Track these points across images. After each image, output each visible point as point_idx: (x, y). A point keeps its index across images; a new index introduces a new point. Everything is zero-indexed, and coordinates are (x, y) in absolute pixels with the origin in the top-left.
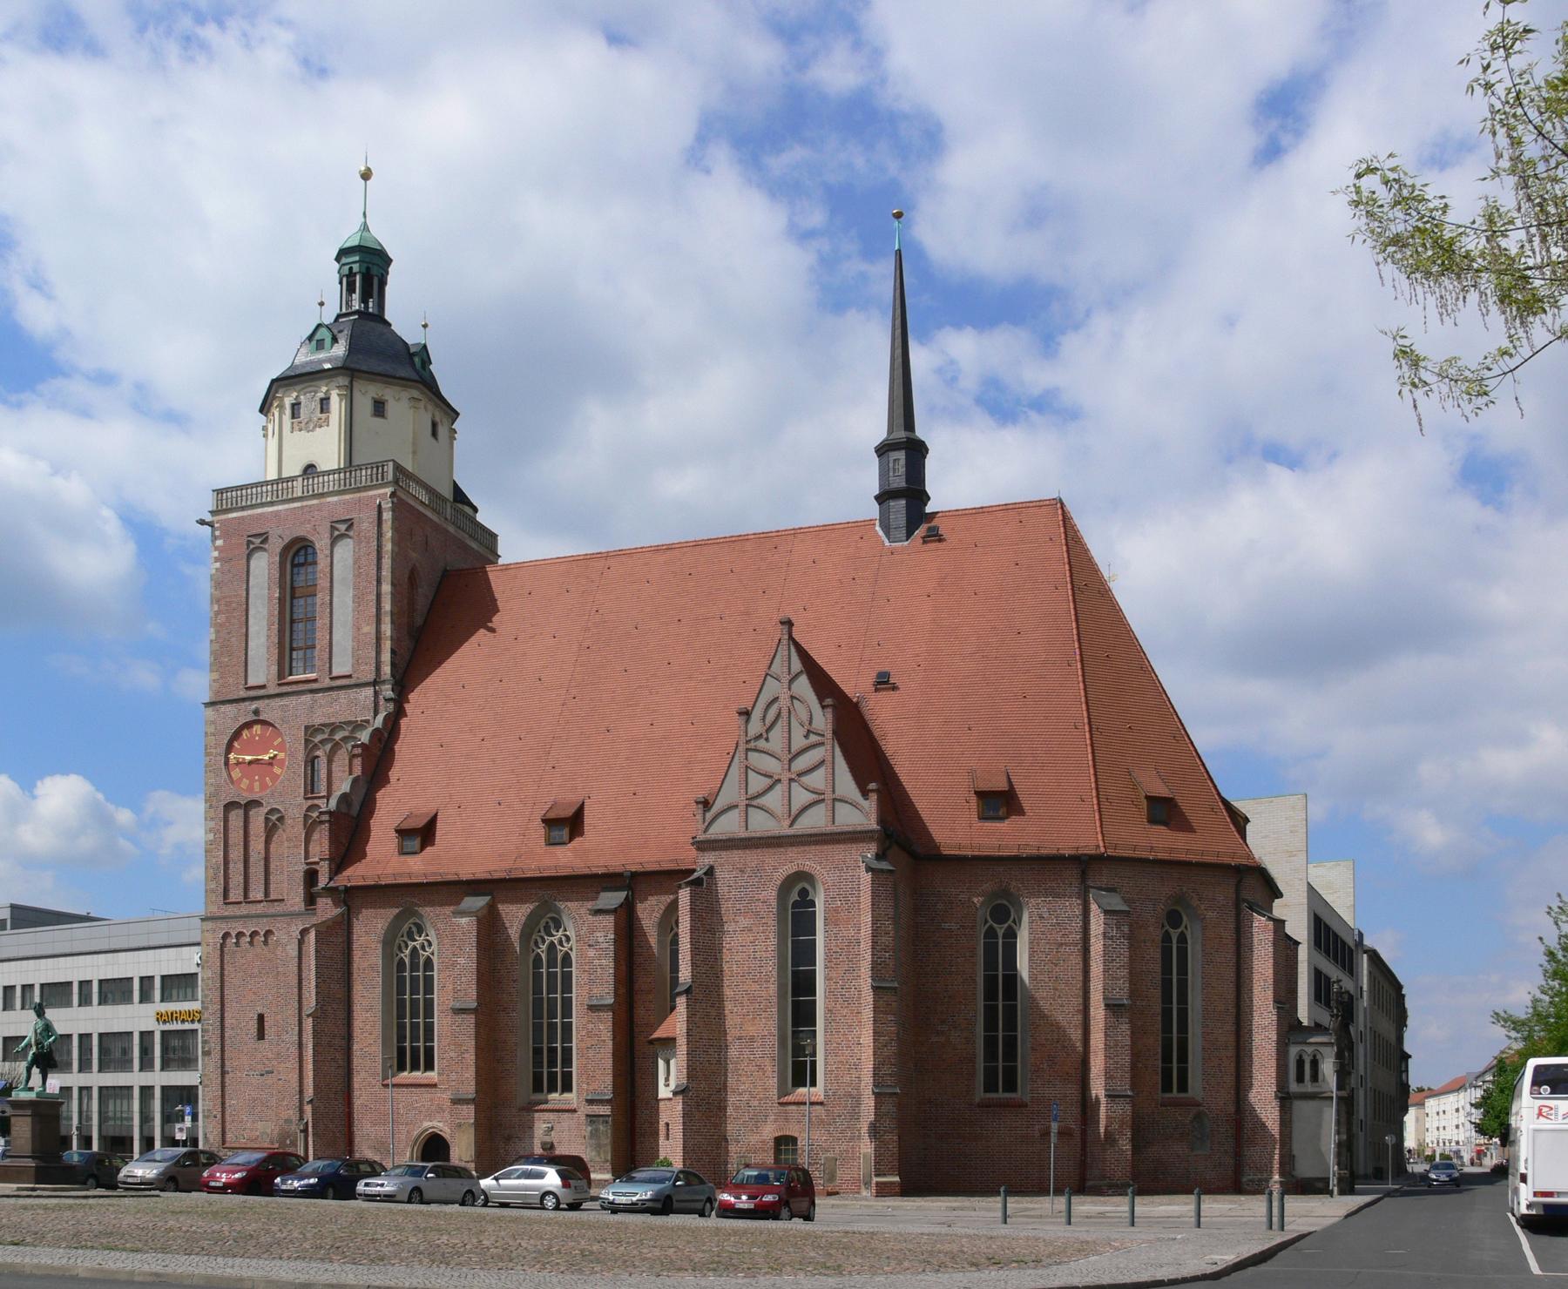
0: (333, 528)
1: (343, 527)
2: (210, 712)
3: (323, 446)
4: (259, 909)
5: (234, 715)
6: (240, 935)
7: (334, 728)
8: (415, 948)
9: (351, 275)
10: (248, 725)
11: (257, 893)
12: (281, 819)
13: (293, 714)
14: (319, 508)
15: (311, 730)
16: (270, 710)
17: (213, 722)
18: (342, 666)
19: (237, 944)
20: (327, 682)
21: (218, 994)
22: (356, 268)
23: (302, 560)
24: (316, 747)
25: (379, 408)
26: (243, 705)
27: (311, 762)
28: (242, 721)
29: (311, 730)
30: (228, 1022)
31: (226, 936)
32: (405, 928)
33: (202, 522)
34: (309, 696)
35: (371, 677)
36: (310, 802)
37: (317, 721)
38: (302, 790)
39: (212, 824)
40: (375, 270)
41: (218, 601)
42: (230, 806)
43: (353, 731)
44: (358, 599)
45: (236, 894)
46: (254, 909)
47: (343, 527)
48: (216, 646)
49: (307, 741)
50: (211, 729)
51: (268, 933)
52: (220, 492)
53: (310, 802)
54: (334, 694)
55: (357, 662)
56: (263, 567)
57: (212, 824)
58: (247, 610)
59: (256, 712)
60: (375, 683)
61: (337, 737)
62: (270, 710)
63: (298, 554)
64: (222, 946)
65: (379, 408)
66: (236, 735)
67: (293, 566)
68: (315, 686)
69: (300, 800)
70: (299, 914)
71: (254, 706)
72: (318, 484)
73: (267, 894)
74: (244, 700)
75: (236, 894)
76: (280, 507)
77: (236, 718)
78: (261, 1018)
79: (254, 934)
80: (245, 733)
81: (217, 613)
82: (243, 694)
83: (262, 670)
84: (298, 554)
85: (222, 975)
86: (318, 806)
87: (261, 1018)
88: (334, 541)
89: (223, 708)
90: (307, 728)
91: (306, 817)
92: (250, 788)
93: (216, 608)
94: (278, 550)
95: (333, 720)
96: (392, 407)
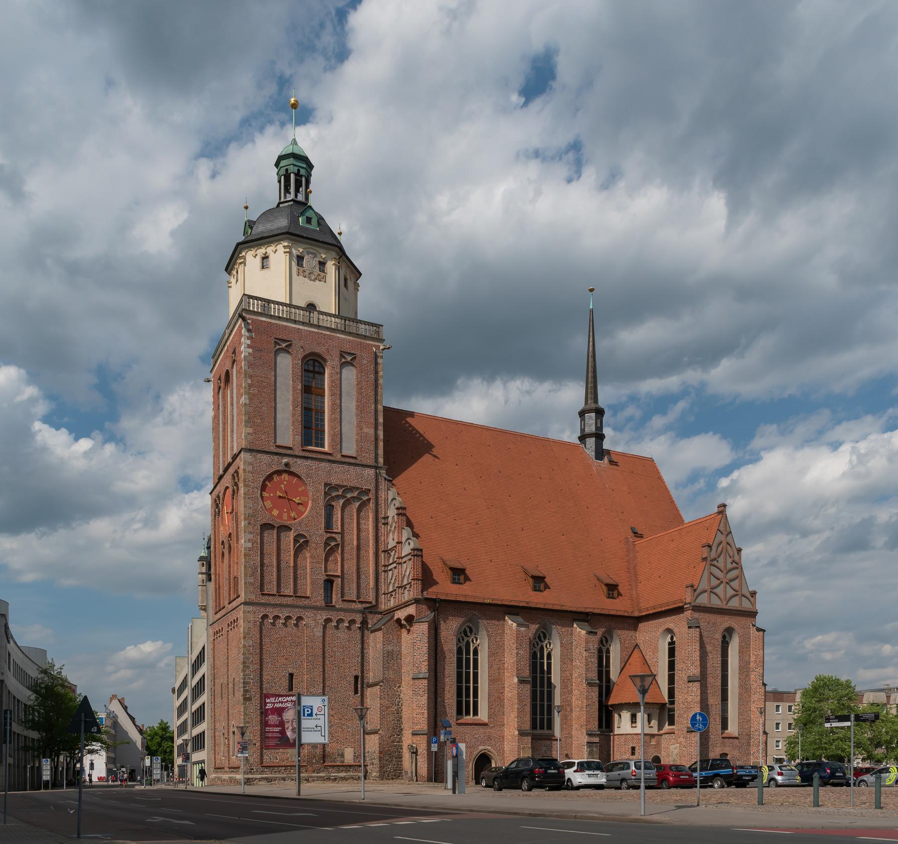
1: (349, 358)
4: (289, 601)
6: (276, 617)
10: (279, 473)
11: (289, 591)
13: (315, 476)
17: (250, 464)
18: (350, 448)
19: (273, 624)
21: (257, 657)
24: (333, 499)
27: (329, 508)
28: (275, 468)
30: (265, 677)
31: (265, 617)
34: (327, 464)
36: (329, 535)
37: (334, 481)
38: (323, 525)
41: (251, 377)
42: (266, 527)
44: (361, 409)
45: (271, 588)
46: (285, 601)
50: (250, 468)
51: (300, 619)
53: (329, 535)
54: (346, 467)
55: (360, 450)
57: (251, 536)
58: (275, 390)
59: (287, 465)
61: (349, 495)
62: (299, 466)
64: (262, 624)
66: (269, 478)
71: (285, 460)
73: (295, 591)
74: (277, 454)
75: (271, 588)
77: (270, 465)
78: (291, 675)
79: (288, 618)
80: (276, 478)
85: (261, 644)
86: (335, 539)
87: (291, 675)
89: (259, 455)
91: (326, 544)
92: (280, 516)
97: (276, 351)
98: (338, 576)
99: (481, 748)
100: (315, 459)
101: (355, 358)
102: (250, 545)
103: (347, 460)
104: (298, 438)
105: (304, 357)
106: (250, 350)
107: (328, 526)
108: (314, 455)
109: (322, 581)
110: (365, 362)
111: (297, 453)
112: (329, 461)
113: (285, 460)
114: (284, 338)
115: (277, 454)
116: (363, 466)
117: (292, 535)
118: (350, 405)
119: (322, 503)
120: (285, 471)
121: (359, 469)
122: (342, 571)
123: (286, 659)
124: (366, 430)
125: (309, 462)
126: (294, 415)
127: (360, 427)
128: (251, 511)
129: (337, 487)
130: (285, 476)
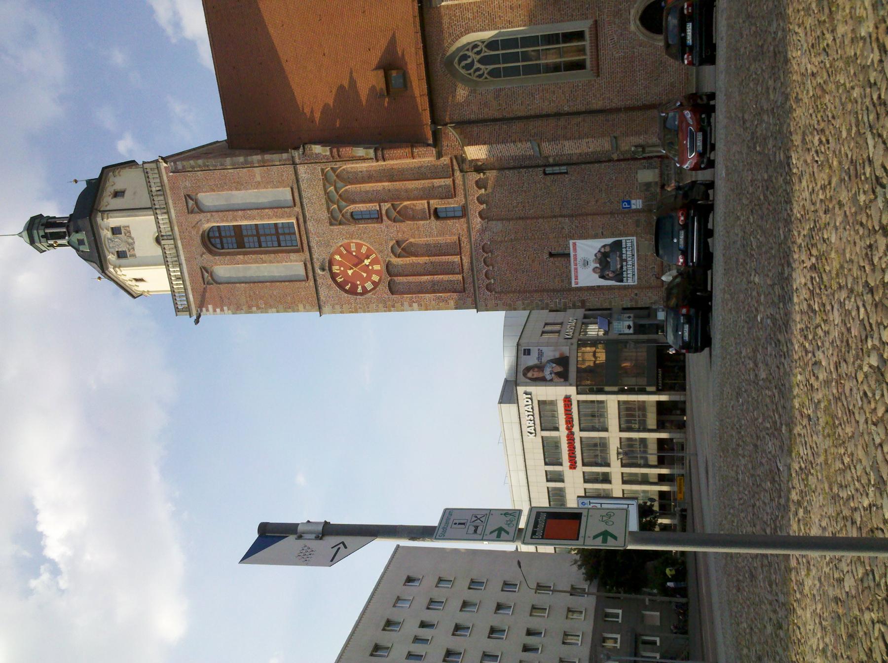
0: (192, 212)
1: (191, 203)
2: (325, 309)
3: (142, 228)
5: (327, 290)
7: (329, 199)
8: (479, 61)
9: (47, 237)
10: (333, 276)
12: (398, 243)
14: (180, 225)
15: (333, 220)
16: (320, 254)
17: (333, 307)
20: (298, 209)
22: (42, 233)
23: (218, 241)
25: (118, 194)
26: (319, 281)
27: (356, 218)
28: (330, 281)
29: (333, 220)
31: (489, 288)
32: (463, 72)
33: (197, 321)
35: (290, 169)
36: (385, 218)
37: (325, 215)
39: (406, 304)
40: (44, 221)
41: (250, 307)
43: (331, 184)
47: (191, 203)
48: (281, 307)
49: (340, 224)
50: (338, 307)
52: (177, 310)
53: (385, 218)
54: (305, 201)
56: (224, 269)
57: (406, 304)
60: (294, 164)
63: (214, 242)
65: (118, 194)
67: (223, 248)
68: (301, 220)
69: (383, 226)
70: (468, 223)
71: (319, 272)
72: (165, 228)
74: (315, 280)
76: (182, 258)
78: (551, 255)
81: (258, 308)
82: (312, 283)
83: (293, 266)
84: (214, 242)
86: (387, 211)
87: (551, 255)
88: (199, 209)
89: (322, 298)
90: (331, 224)
91: (395, 221)
93: (254, 309)
94: (211, 257)
95: (324, 201)
96: (119, 187)
97: (217, 283)
98: (428, 203)
99: (633, 27)
100: (308, 238)
101: (189, 196)
102: (415, 305)
103: (297, 198)
104: (293, 256)
105: (210, 252)
106: (225, 308)
107: (377, 218)
108: (304, 238)
109: (438, 223)
110: (188, 184)
111: (308, 257)
112: (305, 222)
113: (319, 272)
114: (200, 275)
115: (315, 280)
116: (298, 181)
117: (395, 260)
118: (240, 197)
119: (352, 228)
120: (330, 270)
121: (303, 186)
122: (422, 199)
123: (533, 261)
124: (258, 178)
125: (313, 244)
126: (271, 262)
127: (258, 185)
128: (381, 305)
129: (331, 212)
130: (336, 269)
